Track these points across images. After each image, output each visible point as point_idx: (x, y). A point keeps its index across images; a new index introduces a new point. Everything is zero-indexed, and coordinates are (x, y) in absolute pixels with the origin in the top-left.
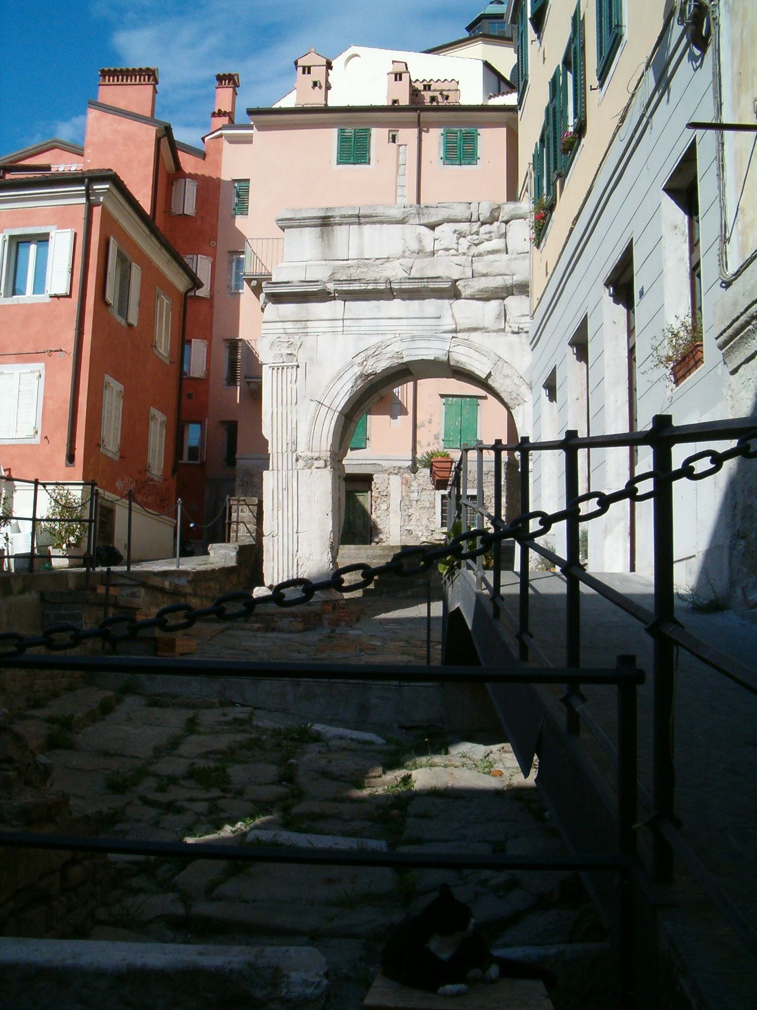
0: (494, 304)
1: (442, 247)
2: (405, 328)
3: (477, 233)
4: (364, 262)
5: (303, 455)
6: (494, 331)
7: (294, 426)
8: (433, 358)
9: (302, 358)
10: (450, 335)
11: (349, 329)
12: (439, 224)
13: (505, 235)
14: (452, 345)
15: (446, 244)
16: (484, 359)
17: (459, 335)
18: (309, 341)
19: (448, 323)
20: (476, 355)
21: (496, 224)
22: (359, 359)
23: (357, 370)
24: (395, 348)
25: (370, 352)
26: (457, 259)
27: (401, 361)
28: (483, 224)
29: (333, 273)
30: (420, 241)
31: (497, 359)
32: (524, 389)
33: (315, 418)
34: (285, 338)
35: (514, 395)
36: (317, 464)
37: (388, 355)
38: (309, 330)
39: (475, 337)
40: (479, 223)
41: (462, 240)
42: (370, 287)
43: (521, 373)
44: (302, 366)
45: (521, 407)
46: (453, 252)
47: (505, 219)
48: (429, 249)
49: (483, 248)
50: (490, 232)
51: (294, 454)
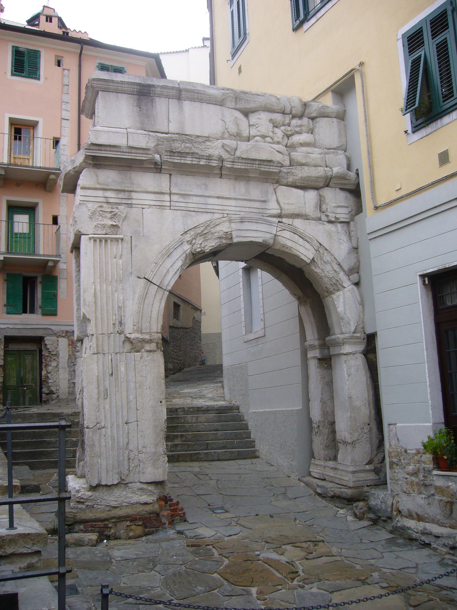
0: (311, 195)
1: (259, 134)
2: (233, 209)
3: (289, 125)
4: (184, 137)
5: (132, 336)
6: (314, 219)
8: (261, 241)
9: (126, 231)
10: (276, 220)
11: (177, 204)
12: (254, 111)
14: (279, 229)
16: (308, 246)
17: (284, 220)
18: (134, 211)
19: (273, 208)
20: (301, 241)
21: (305, 120)
22: (188, 237)
23: (187, 247)
24: (224, 228)
25: (199, 231)
26: (276, 146)
27: (229, 242)
28: (294, 117)
29: (157, 145)
30: (238, 125)
32: (342, 276)
33: (144, 297)
34: (107, 208)
35: (334, 281)
36: (147, 347)
37: (217, 235)
38: (134, 202)
39: (298, 223)
40: (291, 116)
41: (276, 130)
42: (202, 162)
44: (128, 239)
45: (341, 293)
46: (268, 139)
47: (314, 115)
48: (245, 134)
49: (296, 139)
50: (301, 126)
51: (123, 335)
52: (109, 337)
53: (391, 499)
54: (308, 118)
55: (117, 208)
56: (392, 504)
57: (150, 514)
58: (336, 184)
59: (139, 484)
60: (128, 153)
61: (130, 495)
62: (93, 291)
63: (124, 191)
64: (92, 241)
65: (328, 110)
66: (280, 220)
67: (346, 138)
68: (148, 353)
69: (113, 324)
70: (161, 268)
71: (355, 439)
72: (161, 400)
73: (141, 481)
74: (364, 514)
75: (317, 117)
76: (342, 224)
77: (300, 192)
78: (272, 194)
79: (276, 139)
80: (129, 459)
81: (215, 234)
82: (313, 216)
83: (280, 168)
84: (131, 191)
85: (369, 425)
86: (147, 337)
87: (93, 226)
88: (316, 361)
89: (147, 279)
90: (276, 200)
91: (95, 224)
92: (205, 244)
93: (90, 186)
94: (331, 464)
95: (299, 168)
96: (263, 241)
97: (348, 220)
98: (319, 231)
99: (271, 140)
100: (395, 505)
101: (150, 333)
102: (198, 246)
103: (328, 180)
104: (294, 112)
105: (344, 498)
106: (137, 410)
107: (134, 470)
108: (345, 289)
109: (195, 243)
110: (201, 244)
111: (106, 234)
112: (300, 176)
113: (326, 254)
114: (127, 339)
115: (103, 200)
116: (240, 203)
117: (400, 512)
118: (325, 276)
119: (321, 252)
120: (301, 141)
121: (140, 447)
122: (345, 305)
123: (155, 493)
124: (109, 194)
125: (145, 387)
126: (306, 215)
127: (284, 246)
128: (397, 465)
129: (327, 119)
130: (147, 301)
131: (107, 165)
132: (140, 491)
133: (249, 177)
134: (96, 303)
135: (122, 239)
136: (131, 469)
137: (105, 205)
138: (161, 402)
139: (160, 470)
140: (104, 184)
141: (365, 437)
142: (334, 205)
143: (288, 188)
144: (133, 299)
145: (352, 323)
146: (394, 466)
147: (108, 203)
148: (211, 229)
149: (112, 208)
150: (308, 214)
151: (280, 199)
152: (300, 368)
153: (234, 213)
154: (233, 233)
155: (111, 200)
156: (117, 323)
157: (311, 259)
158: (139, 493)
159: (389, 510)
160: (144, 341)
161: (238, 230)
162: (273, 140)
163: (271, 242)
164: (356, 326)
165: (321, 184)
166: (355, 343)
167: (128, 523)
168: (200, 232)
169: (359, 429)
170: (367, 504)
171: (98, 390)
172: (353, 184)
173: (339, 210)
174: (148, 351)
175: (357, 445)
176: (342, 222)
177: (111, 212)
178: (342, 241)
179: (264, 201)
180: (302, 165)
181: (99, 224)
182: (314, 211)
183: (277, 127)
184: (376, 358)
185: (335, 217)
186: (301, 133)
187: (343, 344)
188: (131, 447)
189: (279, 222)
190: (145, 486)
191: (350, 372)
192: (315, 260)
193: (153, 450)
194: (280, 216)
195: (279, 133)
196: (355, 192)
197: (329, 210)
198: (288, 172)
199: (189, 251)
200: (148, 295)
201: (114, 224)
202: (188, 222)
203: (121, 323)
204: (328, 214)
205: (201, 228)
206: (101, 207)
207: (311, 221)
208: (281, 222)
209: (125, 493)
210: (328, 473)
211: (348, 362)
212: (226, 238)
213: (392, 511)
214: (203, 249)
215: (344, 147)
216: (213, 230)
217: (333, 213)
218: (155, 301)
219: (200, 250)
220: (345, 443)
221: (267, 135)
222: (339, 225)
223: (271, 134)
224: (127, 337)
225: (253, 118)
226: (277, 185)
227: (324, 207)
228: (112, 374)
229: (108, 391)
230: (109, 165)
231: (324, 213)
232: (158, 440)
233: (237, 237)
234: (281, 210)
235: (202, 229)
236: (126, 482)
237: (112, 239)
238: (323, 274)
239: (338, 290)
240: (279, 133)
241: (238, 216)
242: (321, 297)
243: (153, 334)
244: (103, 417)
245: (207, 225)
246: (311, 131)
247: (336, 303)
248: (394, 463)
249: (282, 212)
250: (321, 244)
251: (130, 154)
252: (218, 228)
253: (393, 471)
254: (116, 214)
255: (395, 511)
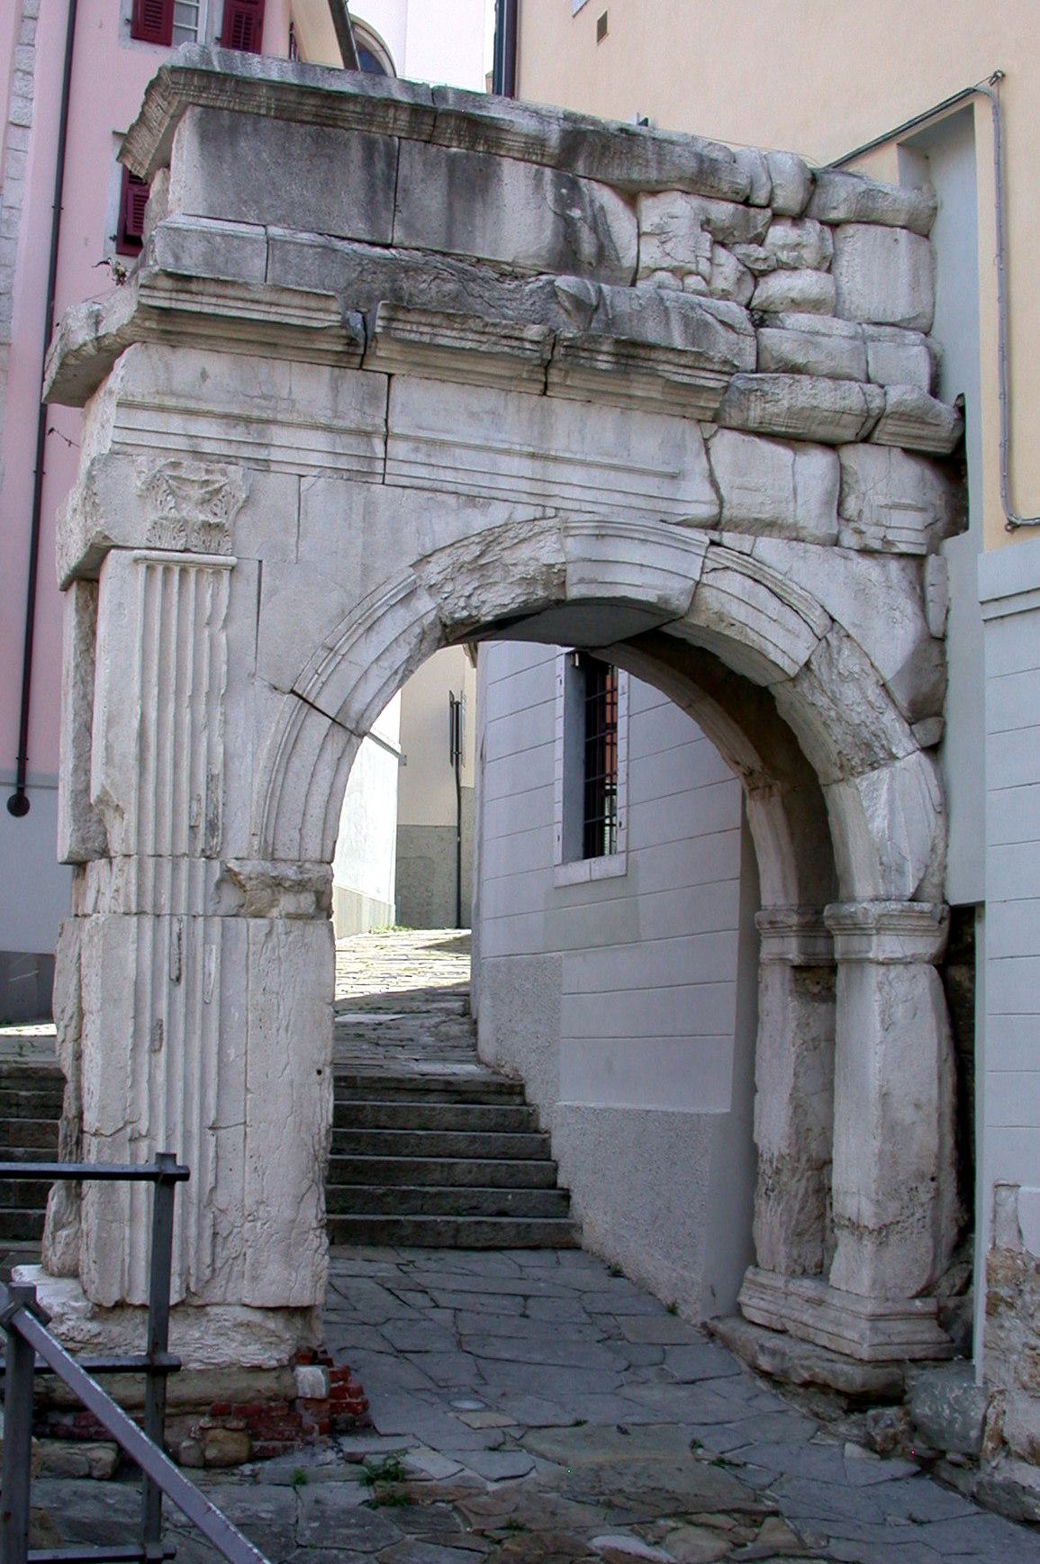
0: (816, 463)
1: (666, 263)
2: (577, 493)
7: (217, 769)
8: (650, 596)
10: (703, 537)
11: (406, 469)
13: (828, 265)
15: (681, 253)
16: (793, 621)
17: (728, 538)
20: (773, 605)
21: (812, 227)
24: (547, 551)
27: (555, 594)
28: (777, 216)
31: (828, 622)
33: (287, 750)
36: (287, 903)
37: (518, 572)
38: (276, 455)
39: (769, 548)
40: (768, 212)
41: (722, 253)
43: (888, 675)
44: (250, 569)
45: (884, 774)
46: (693, 282)
49: (777, 286)
51: (216, 864)
52: (175, 868)
53: (983, 1405)
54: (822, 223)
55: (224, 473)
56: (985, 1418)
57: (269, 1399)
58: (893, 434)
59: (238, 1309)
60: (271, 304)
61: (209, 1340)
62: (136, 724)
63: (248, 421)
64: (142, 568)
65: (882, 204)
66: (715, 536)
67: (934, 295)
68: (288, 922)
69: (192, 827)
70: (343, 666)
71: (887, 1221)
72: (319, 1066)
73: (247, 1301)
74: (896, 1443)
75: (848, 222)
76: (903, 562)
77: (783, 454)
78: (698, 456)
79: (720, 284)
80: (215, 1234)
81: (515, 570)
82: (817, 533)
83: (726, 378)
84: (268, 422)
85: (933, 1179)
86: (291, 872)
87: (148, 525)
88: (788, 973)
89: (300, 697)
90: (707, 473)
91: (154, 516)
92: (482, 598)
93: (148, 400)
94: (808, 1287)
95: (785, 379)
96: (660, 598)
97: (923, 550)
98: (828, 580)
99: (702, 286)
100: (991, 1421)
101: (300, 863)
102: (462, 603)
103: (871, 422)
104: (779, 202)
105: (839, 1393)
106: (247, 1090)
107: (227, 1269)
108: (897, 764)
109: (451, 593)
110: (469, 597)
111: (186, 550)
112: (785, 403)
113: (846, 652)
114: (230, 877)
115: (182, 444)
116: (600, 477)
117: (1004, 1442)
118: (839, 719)
119: (834, 642)
120: (793, 295)
121: (248, 1201)
122: (892, 811)
123: (283, 1341)
124: (202, 427)
125: (275, 1025)
126: (795, 527)
127: (721, 617)
128: (1011, 1306)
129: (879, 229)
130: (296, 763)
131: (202, 336)
132: (242, 1330)
133: (630, 397)
134: (142, 760)
135: (233, 569)
136: (218, 1265)
137: (187, 461)
138: (319, 1072)
139: (306, 1273)
140: (190, 397)
141: (918, 1215)
142: (883, 501)
143: (746, 438)
144: (254, 754)
145: (910, 868)
146: (1002, 1308)
147: (197, 454)
148: (506, 553)
149: (208, 472)
150: (801, 524)
151: (718, 474)
152: (733, 987)
153: (576, 506)
154: (570, 568)
155: (207, 447)
156: (202, 826)
157: (802, 663)
158: (239, 1337)
159: (974, 1433)
160: (277, 883)
161: (584, 560)
162: (708, 282)
163: (680, 602)
164: (922, 880)
165: (848, 434)
166: (913, 931)
167: (205, 1421)
168: (467, 558)
169: (903, 1190)
170: (907, 1413)
171: (136, 1025)
172: (946, 441)
173: (897, 518)
174: (289, 916)
175: (894, 1239)
176: (902, 555)
177: (206, 482)
178: (897, 614)
179: (673, 477)
180: (794, 369)
181: (166, 518)
182: (821, 516)
183: (723, 245)
184: (972, 979)
185: (884, 540)
186: (795, 269)
187: (879, 930)
188: (222, 1199)
189: (713, 543)
190: (256, 1317)
191: (888, 1014)
192: (814, 666)
193: (288, 1214)
194: (715, 524)
195: (728, 263)
196: (950, 465)
197: (866, 514)
198: (751, 391)
199: (432, 616)
200: (299, 746)
201: (213, 520)
202: (436, 528)
203: (212, 826)
204: (863, 528)
205: (473, 547)
206: (176, 465)
207: (810, 547)
208: (719, 545)
209: (197, 1335)
210: (796, 1315)
211: (886, 988)
212: (546, 586)
213: (981, 1437)
214: (474, 613)
215: (923, 322)
216: (509, 557)
217: (877, 524)
218: (321, 766)
219: (465, 613)
220: (855, 1227)
221: (693, 267)
222: (894, 566)
223: (704, 266)
224: (229, 870)
225: (653, 211)
226: (715, 426)
227: (851, 505)
228: (178, 979)
229: (165, 1027)
230: (209, 337)
231: (852, 525)
232: (306, 1184)
233: (581, 581)
234: (721, 506)
235: (477, 550)
236: (200, 1302)
237: (201, 567)
238: (833, 714)
239: (873, 766)
240: (728, 263)
241: (588, 517)
242: (821, 781)
243: (308, 865)
244: (144, 1106)
245: (491, 539)
246: (828, 265)
247: (865, 804)
248: (1002, 1299)
249: (726, 513)
250: (833, 620)
251: (274, 309)
252: (525, 552)
253: (996, 1322)
254: (218, 491)
255: (991, 1438)
